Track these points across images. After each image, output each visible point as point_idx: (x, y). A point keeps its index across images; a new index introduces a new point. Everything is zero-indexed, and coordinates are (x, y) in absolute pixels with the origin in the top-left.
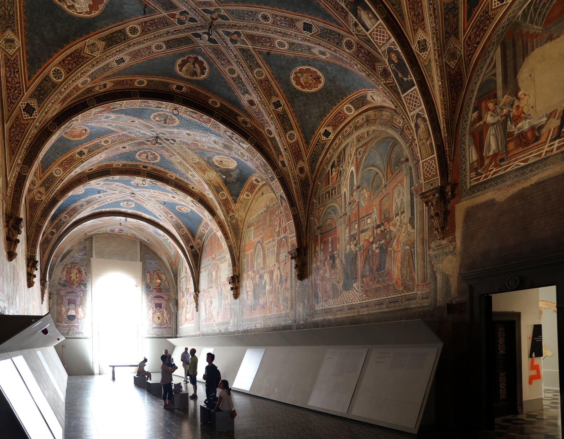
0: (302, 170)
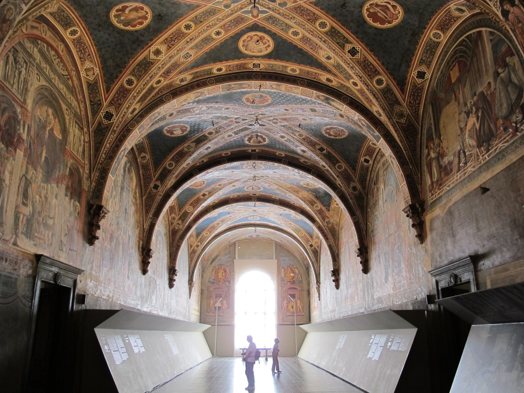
0: (354, 188)
